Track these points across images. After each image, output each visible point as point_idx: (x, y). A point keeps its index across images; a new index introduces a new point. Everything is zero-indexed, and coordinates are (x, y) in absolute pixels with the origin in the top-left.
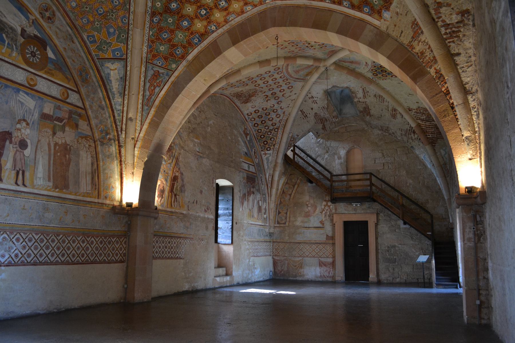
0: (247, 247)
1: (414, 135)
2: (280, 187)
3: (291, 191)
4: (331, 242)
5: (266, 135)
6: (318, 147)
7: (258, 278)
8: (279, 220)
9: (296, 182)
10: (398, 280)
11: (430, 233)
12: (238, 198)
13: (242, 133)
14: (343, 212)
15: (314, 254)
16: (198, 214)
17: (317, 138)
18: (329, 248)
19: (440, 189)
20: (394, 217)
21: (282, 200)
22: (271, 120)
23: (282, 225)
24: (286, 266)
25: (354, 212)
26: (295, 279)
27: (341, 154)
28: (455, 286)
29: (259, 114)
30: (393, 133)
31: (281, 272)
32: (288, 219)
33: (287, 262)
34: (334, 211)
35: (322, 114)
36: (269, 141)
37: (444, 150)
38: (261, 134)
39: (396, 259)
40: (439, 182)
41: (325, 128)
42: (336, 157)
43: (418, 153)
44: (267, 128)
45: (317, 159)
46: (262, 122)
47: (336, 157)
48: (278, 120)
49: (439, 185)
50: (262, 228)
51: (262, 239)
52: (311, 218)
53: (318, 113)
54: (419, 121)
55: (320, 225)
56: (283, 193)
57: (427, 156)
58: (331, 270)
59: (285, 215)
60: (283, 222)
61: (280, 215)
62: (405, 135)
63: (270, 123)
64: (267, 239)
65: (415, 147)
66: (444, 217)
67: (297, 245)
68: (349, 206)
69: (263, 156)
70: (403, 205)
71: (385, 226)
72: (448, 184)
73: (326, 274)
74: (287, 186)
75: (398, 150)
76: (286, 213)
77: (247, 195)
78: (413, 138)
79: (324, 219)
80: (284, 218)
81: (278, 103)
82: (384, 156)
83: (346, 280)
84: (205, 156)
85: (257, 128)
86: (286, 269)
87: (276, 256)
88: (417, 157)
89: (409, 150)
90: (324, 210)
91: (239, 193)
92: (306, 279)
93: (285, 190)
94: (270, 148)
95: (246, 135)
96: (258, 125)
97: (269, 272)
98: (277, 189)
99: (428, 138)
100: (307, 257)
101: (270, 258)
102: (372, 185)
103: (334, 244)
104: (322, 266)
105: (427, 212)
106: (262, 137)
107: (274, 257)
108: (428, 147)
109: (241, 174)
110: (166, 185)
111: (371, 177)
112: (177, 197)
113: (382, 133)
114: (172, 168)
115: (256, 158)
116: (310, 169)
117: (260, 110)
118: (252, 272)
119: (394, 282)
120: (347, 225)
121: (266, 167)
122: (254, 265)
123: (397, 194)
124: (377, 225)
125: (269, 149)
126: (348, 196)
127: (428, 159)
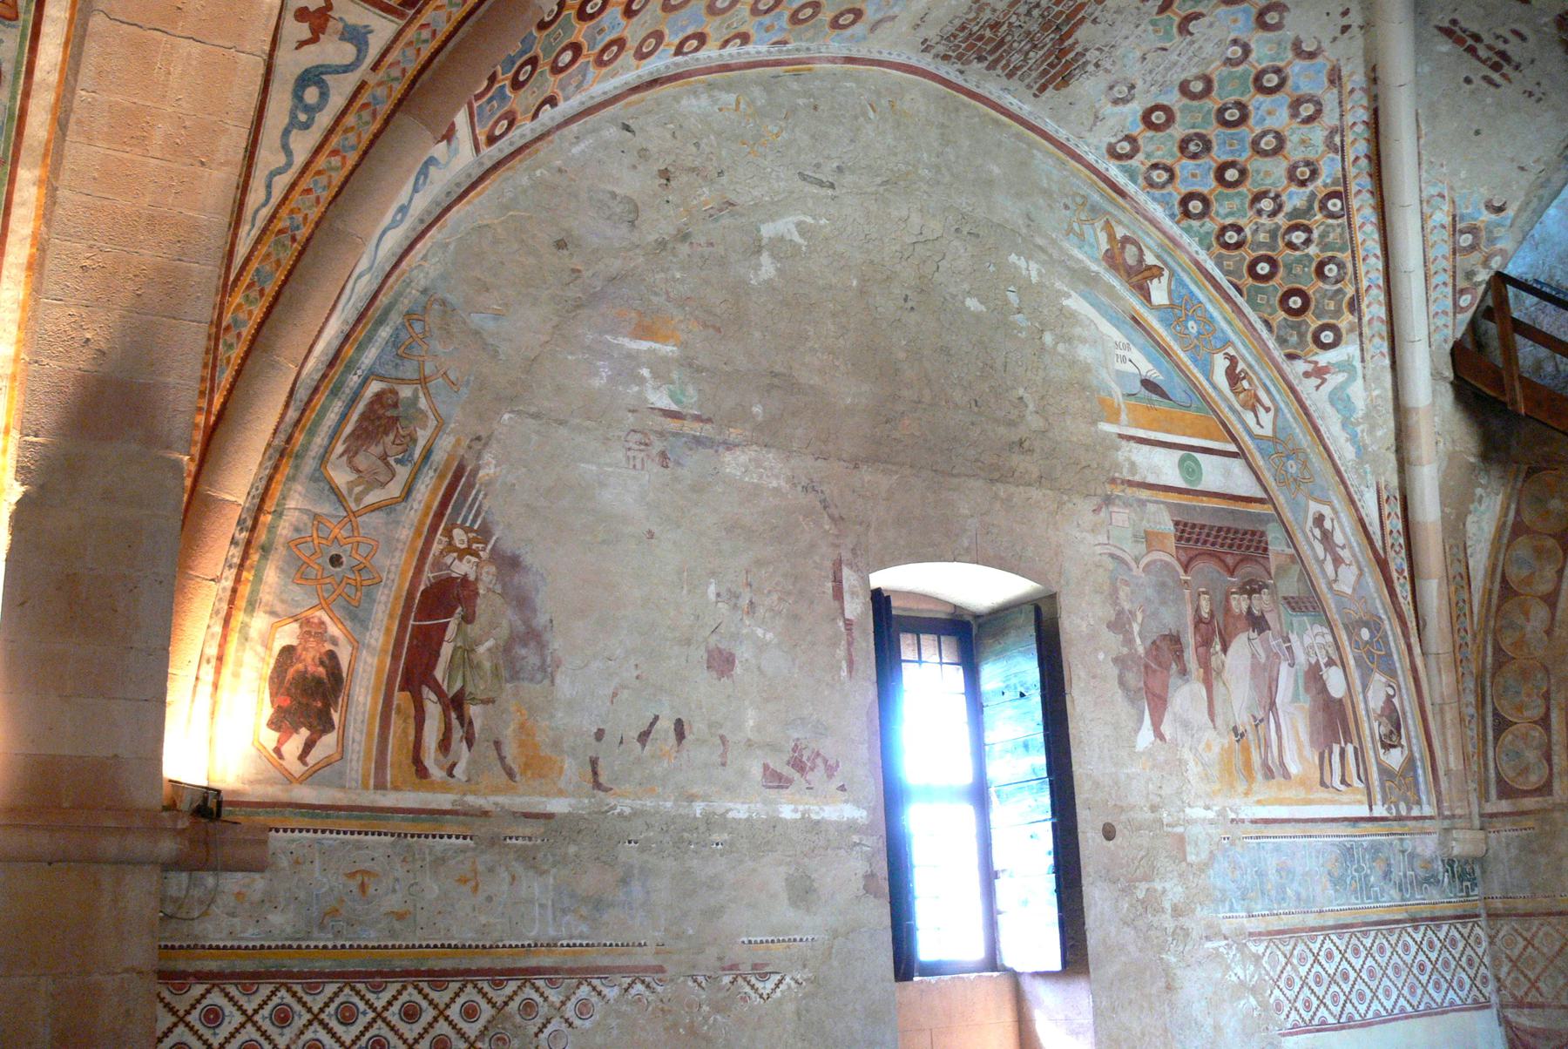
0: (1241, 972)
2: (1479, 562)
5: (1283, 255)
8: (1509, 774)
12: (1113, 671)
16: (698, 808)
21: (1506, 644)
22: (1278, 150)
23: (1529, 803)
29: (1178, 131)
36: (1313, 287)
38: (1248, 254)
46: (1220, 178)
48: (1317, 134)
50: (1368, 836)
51: (1387, 901)
59: (1537, 732)
60: (1534, 779)
61: (1507, 737)
69: (1307, 388)
74: (1523, 548)
76: (1545, 722)
77: (1190, 639)
80: (1531, 756)
81: (1262, 25)
84: (734, 434)
87: (1519, 1004)
91: (1113, 641)
93: (1516, 574)
95: (1140, 276)
96: (1205, 200)
98: (1460, 579)
101: (1490, 1016)
106: (1263, 268)
109: (1121, 516)
110: (357, 645)
112: (473, 711)
114: (405, 533)
115: (1253, 404)
117: (1173, 99)
121: (1345, 452)
125: (1327, 337)
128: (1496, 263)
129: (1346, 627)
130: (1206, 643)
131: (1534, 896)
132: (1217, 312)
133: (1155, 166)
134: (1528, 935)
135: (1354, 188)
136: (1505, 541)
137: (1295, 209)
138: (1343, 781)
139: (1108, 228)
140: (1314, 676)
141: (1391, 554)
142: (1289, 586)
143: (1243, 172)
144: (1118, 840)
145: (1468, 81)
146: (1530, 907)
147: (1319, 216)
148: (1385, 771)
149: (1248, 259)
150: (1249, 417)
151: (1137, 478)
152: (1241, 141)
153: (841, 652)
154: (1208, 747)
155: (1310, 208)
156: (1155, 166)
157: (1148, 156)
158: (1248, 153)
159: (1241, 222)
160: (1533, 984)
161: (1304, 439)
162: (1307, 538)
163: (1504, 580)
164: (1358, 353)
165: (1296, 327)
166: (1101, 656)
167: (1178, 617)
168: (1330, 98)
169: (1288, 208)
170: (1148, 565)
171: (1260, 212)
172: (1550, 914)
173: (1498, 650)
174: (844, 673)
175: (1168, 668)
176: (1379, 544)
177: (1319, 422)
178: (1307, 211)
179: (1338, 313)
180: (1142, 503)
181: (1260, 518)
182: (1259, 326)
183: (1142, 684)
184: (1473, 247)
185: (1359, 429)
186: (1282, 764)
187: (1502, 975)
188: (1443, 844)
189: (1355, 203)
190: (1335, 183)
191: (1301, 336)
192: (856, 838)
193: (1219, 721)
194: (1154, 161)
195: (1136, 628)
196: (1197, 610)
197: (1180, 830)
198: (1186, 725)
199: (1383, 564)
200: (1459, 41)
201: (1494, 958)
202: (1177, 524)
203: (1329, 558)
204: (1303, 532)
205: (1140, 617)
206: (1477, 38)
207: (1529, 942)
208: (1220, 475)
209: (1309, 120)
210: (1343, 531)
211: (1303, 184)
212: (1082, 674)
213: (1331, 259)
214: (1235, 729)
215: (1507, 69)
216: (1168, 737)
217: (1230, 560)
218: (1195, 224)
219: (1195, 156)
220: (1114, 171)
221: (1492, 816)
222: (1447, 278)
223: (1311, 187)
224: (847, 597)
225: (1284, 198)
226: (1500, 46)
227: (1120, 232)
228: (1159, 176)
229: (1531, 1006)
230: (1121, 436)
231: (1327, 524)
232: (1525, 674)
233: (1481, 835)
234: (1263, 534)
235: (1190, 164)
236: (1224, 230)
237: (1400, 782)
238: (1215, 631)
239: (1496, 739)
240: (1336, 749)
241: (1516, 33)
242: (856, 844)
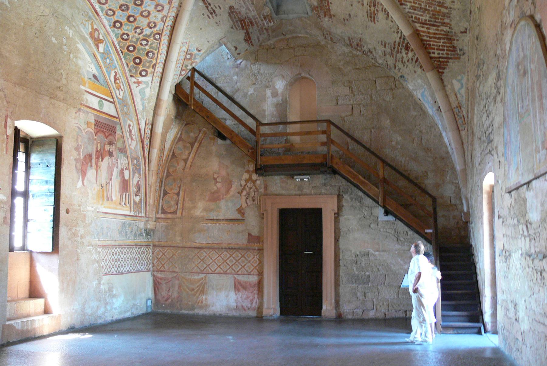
0: (95, 256)
1: (407, 53)
2: (167, 146)
3: (187, 153)
4: (256, 246)
5: (138, 46)
6: (237, 74)
7: (120, 313)
8: (165, 207)
9: (197, 137)
10: (371, 314)
11: (430, 231)
12: (74, 163)
13: (87, 36)
14: (278, 192)
15: (225, 267)
17: (236, 59)
18: (253, 258)
19: (448, 152)
20: (369, 202)
21: (171, 170)
22: (147, 17)
23: (170, 216)
24: (177, 288)
25: (298, 192)
26: (191, 312)
27: (277, 87)
28: (476, 330)
30: (370, 51)
31: (167, 300)
32: (180, 205)
33: (177, 282)
34: (262, 190)
35: (243, 11)
36: (144, 58)
37: (460, 81)
38: (128, 43)
39: (369, 276)
40: (446, 140)
41: (250, 39)
42: (268, 93)
43: (411, 88)
44: (139, 31)
45: (235, 97)
46: (128, 19)
47: (268, 93)
48: (160, 15)
49: (446, 147)
50: (129, 220)
51: (130, 240)
52: (222, 203)
53: (236, 7)
54: (417, 25)
55: (239, 216)
56: (172, 158)
57: (427, 93)
58: (256, 296)
59: (175, 197)
60: (172, 209)
61: (167, 197)
62: (391, 55)
63: (145, 22)
64: (142, 240)
65: (405, 75)
66: (453, 202)
67: (196, 251)
68: (290, 181)
69: (134, 86)
70: (385, 180)
71: (351, 217)
72: (463, 143)
73: (247, 304)
74: (180, 145)
75: (378, 81)
76: (178, 194)
77: (94, 156)
78: (405, 59)
79: (244, 205)
80: (173, 203)
82: (352, 92)
83: (281, 314)
85: (120, 32)
86: (175, 295)
87: (158, 271)
88: (411, 95)
89: (396, 84)
90: (244, 189)
91: (75, 153)
92: (211, 313)
93: (177, 152)
94: (146, 71)
95: (98, 42)
96: (121, 24)
97: (144, 301)
98: (162, 150)
99: (431, 58)
100: (213, 273)
101: (150, 273)
102: (330, 142)
103: (261, 250)
104: (239, 290)
105: (424, 191)
107: (155, 273)
108: (431, 76)
109: (82, 115)
111: (328, 127)
113: (350, 52)
115: (119, 88)
116: (221, 114)
118: (106, 304)
119: (365, 317)
120: (284, 214)
121: (140, 108)
122: (110, 289)
123: (374, 159)
124: (337, 216)
125: (144, 73)
126: (287, 162)
127: (430, 98)
128: (194, 65)
130: (98, 158)
131: (167, 241)
132: (115, 57)
133: (110, 9)
134: (164, 252)
135: (164, 33)
136: (176, 141)
137: (146, 34)
139: (92, 24)
140: (122, 172)
141: (145, 139)
142: (120, 145)
143: (135, 19)
144: (70, 214)
145: (203, 14)
146: (165, 244)
147: (152, 38)
148: (134, 202)
149: (128, 44)
150: (117, 92)
151: (88, 105)
152: (138, 10)
153: (4, 145)
154: (94, 189)
155: (150, 35)
156: (110, 9)
157: (109, 6)
158: (139, 14)
159: (129, 33)
160: (163, 265)
161: (129, 101)
163: (173, 152)
164: (151, 80)
165: (135, 68)
166: (72, 158)
167: (92, 149)
168: (167, 7)
169: (144, 33)
171: (136, 32)
172: (171, 247)
173: (168, 171)
174: (5, 152)
176: (143, 136)
177: (134, 97)
178: (149, 36)
179: (149, 67)
180: (88, 112)
181: (115, 122)
182: (125, 65)
184: (190, 59)
185: (145, 102)
186: (111, 197)
187: (155, 263)
188: (145, 225)
189: (163, 38)
190: (159, 30)
191: (136, 71)
192: (2, 206)
194: (110, 8)
195: (81, 150)
196: (97, 147)
197: (85, 213)
198: (90, 182)
199: (142, 142)
200: (205, 4)
201: (153, 258)
202: (95, 120)
206: (210, 4)
207: (164, 254)
208: (109, 108)
209: (159, 11)
210: (135, 131)
211: (151, 28)
212: (66, 162)
213: (151, 52)
215: (214, 15)
217: (107, 134)
218: (116, 30)
219: (123, 10)
220: (97, 6)
221: (159, 218)
222: (181, 66)
223: (153, 30)
224: (8, 127)
225: (144, 30)
226: (214, 8)
227: (95, 27)
228: (110, 13)
229: (161, 271)
230: (85, 91)
231: (131, 128)
232: (174, 180)
233: (155, 223)
234: (115, 128)
235: (121, 12)
236: (124, 34)
237: (137, 205)
238: (100, 155)
239: (163, 197)
240: (124, 194)
241: (219, 6)
242: (2, 207)
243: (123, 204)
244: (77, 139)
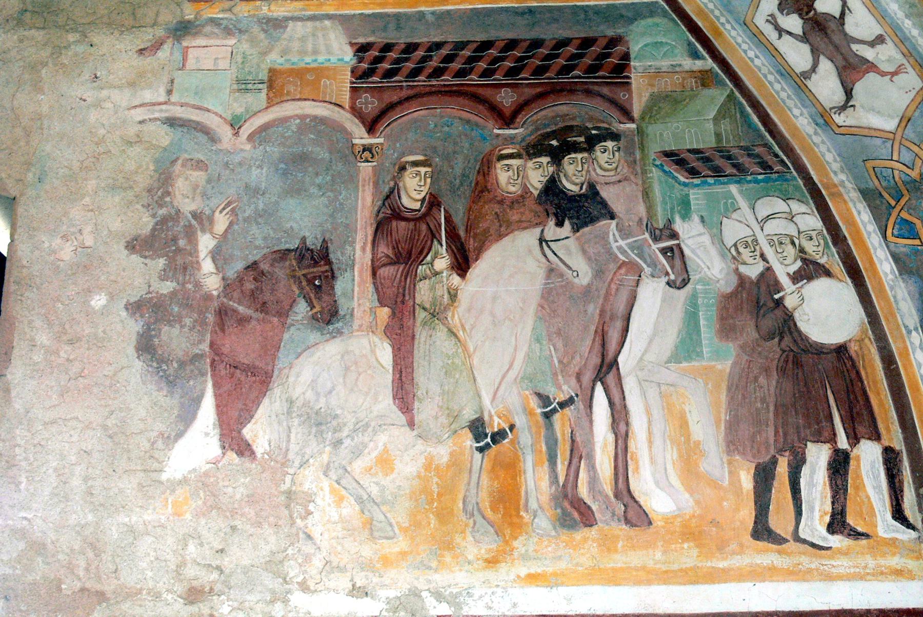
77: (358, 254)
91: (144, 275)
129: (869, 195)
138: (837, 524)
140: (757, 305)
154: (385, 462)
162: (757, 37)
170: (265, 128)
175: (283, 314)
183: (205, 347)
186: (623, 491)
193: (425, 411)
195: (206, 243)
198: (319, 422)
202: (362, 49)
203: (825, 65)
204: (746, 25)
205: (221, 223)
212: (43, 338)
214: (477, 428)
216: (260, 447)
217: (506, 99)
238: (429, 237)
240: (818, 457)
243: (815, 524)
244: (164, 181)
